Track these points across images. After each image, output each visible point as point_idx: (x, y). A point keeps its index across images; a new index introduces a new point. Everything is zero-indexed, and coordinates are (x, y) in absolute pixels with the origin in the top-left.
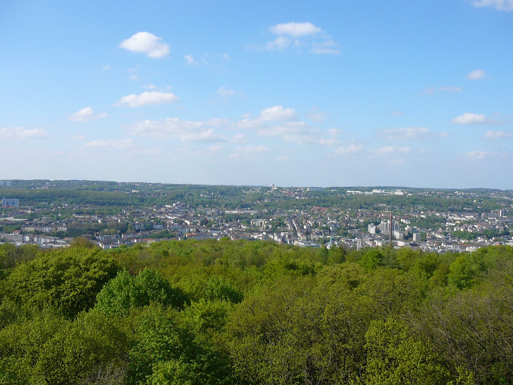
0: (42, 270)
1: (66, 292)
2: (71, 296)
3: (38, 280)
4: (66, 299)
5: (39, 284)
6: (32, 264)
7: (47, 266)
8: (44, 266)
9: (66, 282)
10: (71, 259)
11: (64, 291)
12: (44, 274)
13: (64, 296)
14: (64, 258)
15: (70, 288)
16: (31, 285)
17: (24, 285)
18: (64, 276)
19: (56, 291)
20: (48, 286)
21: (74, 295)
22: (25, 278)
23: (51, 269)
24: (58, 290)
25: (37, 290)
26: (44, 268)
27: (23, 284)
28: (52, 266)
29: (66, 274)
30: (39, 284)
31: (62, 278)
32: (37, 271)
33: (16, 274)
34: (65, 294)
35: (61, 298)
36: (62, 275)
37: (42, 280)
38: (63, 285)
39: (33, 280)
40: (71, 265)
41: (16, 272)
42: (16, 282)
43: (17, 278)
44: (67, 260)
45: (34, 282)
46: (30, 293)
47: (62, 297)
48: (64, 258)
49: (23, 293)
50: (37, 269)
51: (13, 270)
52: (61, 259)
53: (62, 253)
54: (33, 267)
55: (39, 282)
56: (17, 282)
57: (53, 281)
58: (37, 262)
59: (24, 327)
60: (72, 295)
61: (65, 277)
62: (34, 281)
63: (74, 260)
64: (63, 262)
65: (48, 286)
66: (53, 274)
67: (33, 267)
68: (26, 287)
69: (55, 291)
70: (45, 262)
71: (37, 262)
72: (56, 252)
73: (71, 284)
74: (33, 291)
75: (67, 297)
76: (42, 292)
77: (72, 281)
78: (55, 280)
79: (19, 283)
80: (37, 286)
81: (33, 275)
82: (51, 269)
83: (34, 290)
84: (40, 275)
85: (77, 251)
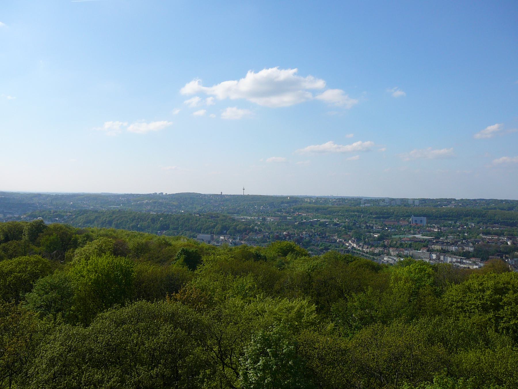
0: (478, 292)
1: (505, 319)
2: (512, 323)
3: (474, 302)
4: (506, 326)
5: (476, 306)
6: (467, 284)
7: (483, 288)
8: (480, 288)
9: (506, 308)
10: (508, 283)
11: (503, 317)
12: (481, 297)
13: (503, 323)
14: (501, 282)
15: (510, 315)
16: (468, 306)
17: (460, 305)
18: (503, 301)
19: (494, 315)
20: (485, 309)
21: (515, 324)
22: (460, 298)
23: (488, 293)
24: (497, 315)
25: (474, 312)
26: (480, 290)
27: (460, 304)
28: (488, 288)
29: (505, 300)
30: (476, 306)
31: (501, 303)
32: (473, 292)
33: (451, 293)
34: (504, 321)
35: (500, 324)
36: (501, 300)
37: (479, 302)
38: (502, 310)
39: (468, 301)
40: (509, 290)
41: (451, 291)
42: (452, 301)
43: (452, 297)
44: (504, 284)
45: (470, 304)
46: (467, 314)
47: (501, 323)
48: (501, 282)
49: (460, 313)
50: (473, 290)
51: (447, 289)
52: (498, 283)
53: (498, 276)
54: (469, 288)
55: (476, 304)
56: (453, 302)
57: (491, 305)
58: (472, 284)
59: (499, 354)
60: (513, 322)
61: (504, 303)
62: (470, 302)
63: (513, 286)
64: (500, 286)
65: (485, 309)
66: (491, 297)
67: (469, 288)
68: (462, 308)
69: (493, 315)
70: (481, 284)
71: (472, 284)
72: (491, 275)
73: (511, 310)
74: (470, 313)
75: (507, 325)
76: (480, 315)
77: (511, 308)
78: (493, 304)
79: (455, 302)
80: (474, 308)
81: (469, 296)
82: (488, 293)
83: (471, 312)
84: (477, 297)
85: (515, 276)
